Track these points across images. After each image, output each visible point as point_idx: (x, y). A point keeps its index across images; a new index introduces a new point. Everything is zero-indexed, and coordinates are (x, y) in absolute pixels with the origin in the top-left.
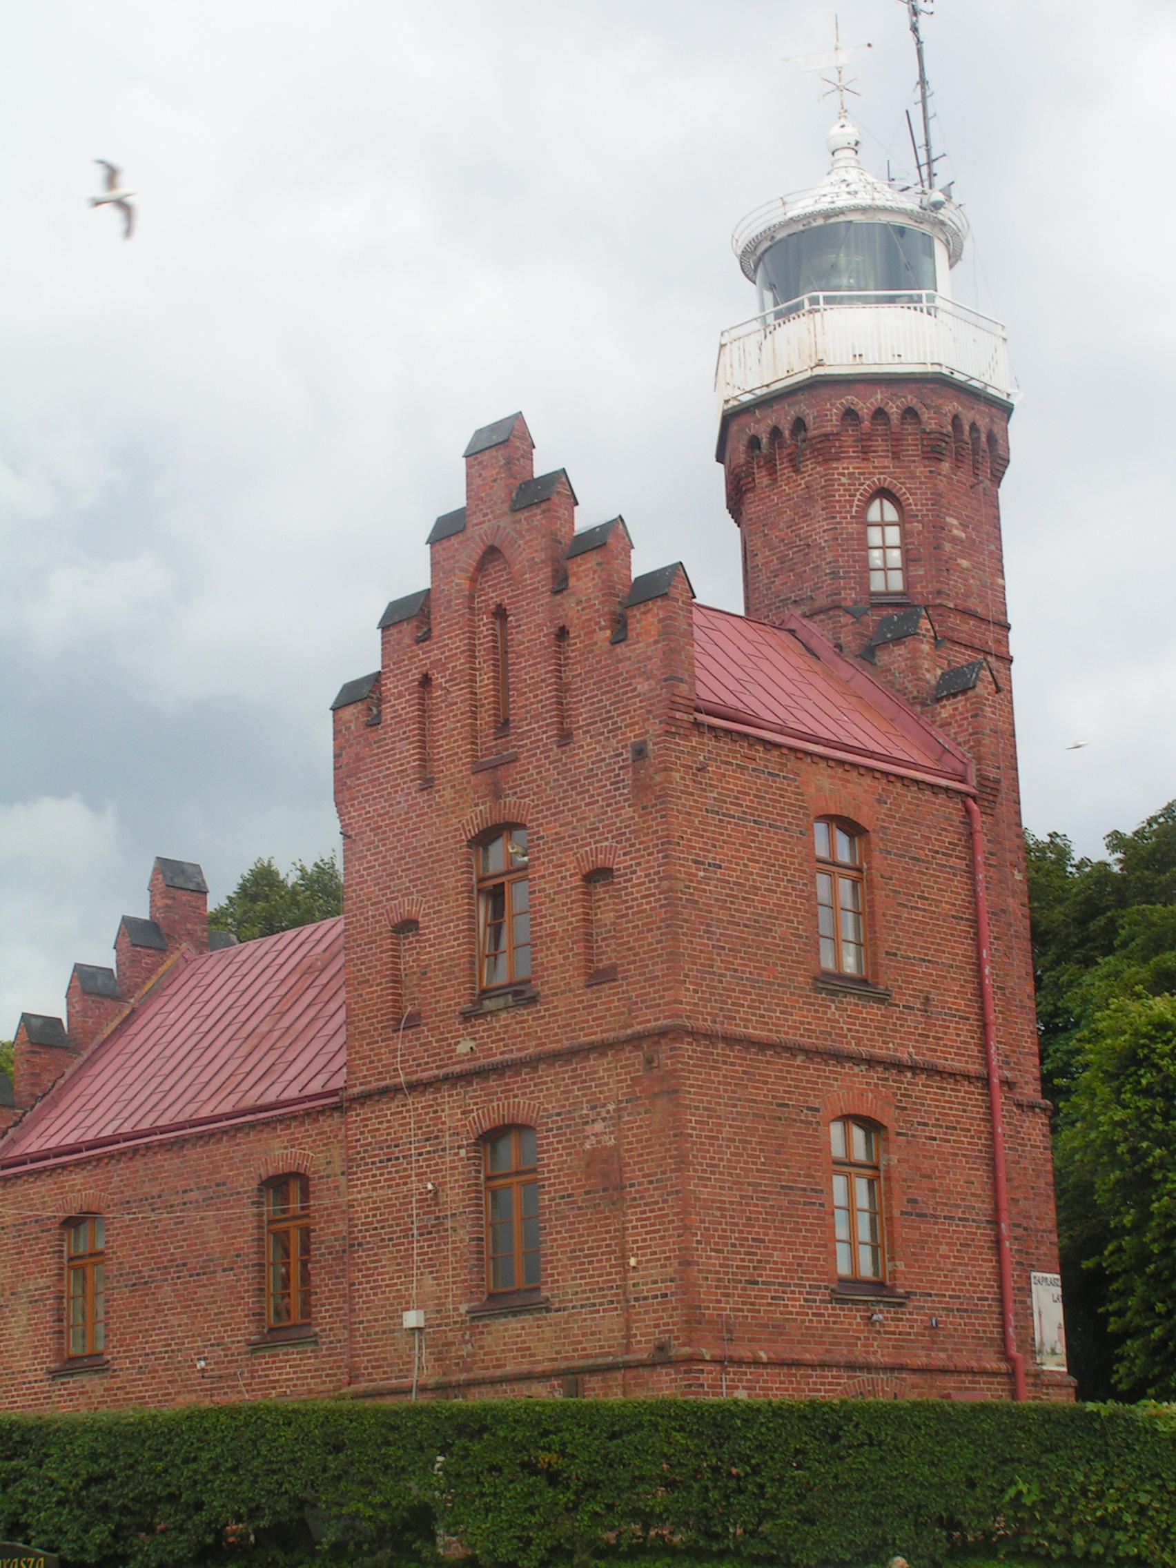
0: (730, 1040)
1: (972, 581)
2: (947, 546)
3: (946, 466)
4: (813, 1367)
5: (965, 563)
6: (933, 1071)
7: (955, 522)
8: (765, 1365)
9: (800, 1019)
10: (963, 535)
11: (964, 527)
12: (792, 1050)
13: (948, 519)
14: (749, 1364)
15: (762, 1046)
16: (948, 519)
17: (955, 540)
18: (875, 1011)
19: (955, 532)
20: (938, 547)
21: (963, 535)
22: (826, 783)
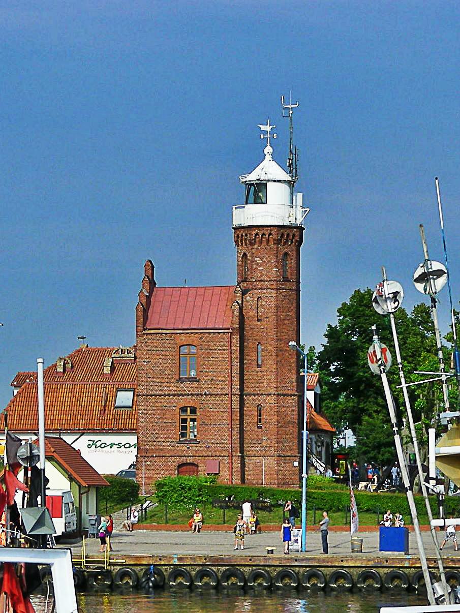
0: (151, 396)
1: (263, 272)
2: (255, 266)
3: (256, 246)
4: (169, 457)
5: (261, 268)
6: (211, 395)
7: (259, 259)
8: (155, 457)
9: (173, 388)
10: (261, 262)
11: (262, 259)
12: (169, 395)
13: (255, 259)
14: (151, 457)
15: (160, 396)
16: (255, 259)
17: (258, 264)
18: (195, 384)
19: (258, 262)
20: (252, 267)
21: (261, 262)
22: (184, 338)
